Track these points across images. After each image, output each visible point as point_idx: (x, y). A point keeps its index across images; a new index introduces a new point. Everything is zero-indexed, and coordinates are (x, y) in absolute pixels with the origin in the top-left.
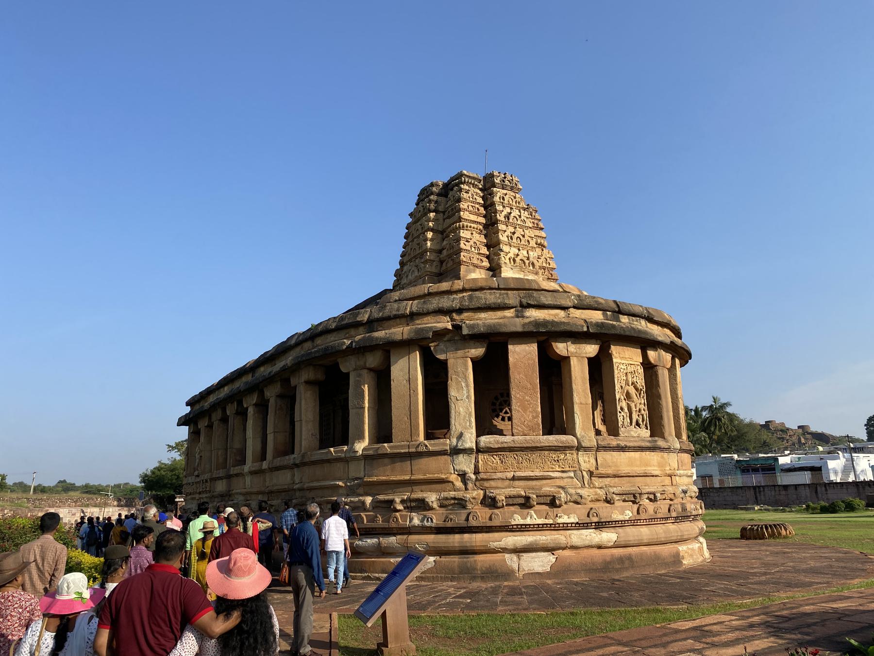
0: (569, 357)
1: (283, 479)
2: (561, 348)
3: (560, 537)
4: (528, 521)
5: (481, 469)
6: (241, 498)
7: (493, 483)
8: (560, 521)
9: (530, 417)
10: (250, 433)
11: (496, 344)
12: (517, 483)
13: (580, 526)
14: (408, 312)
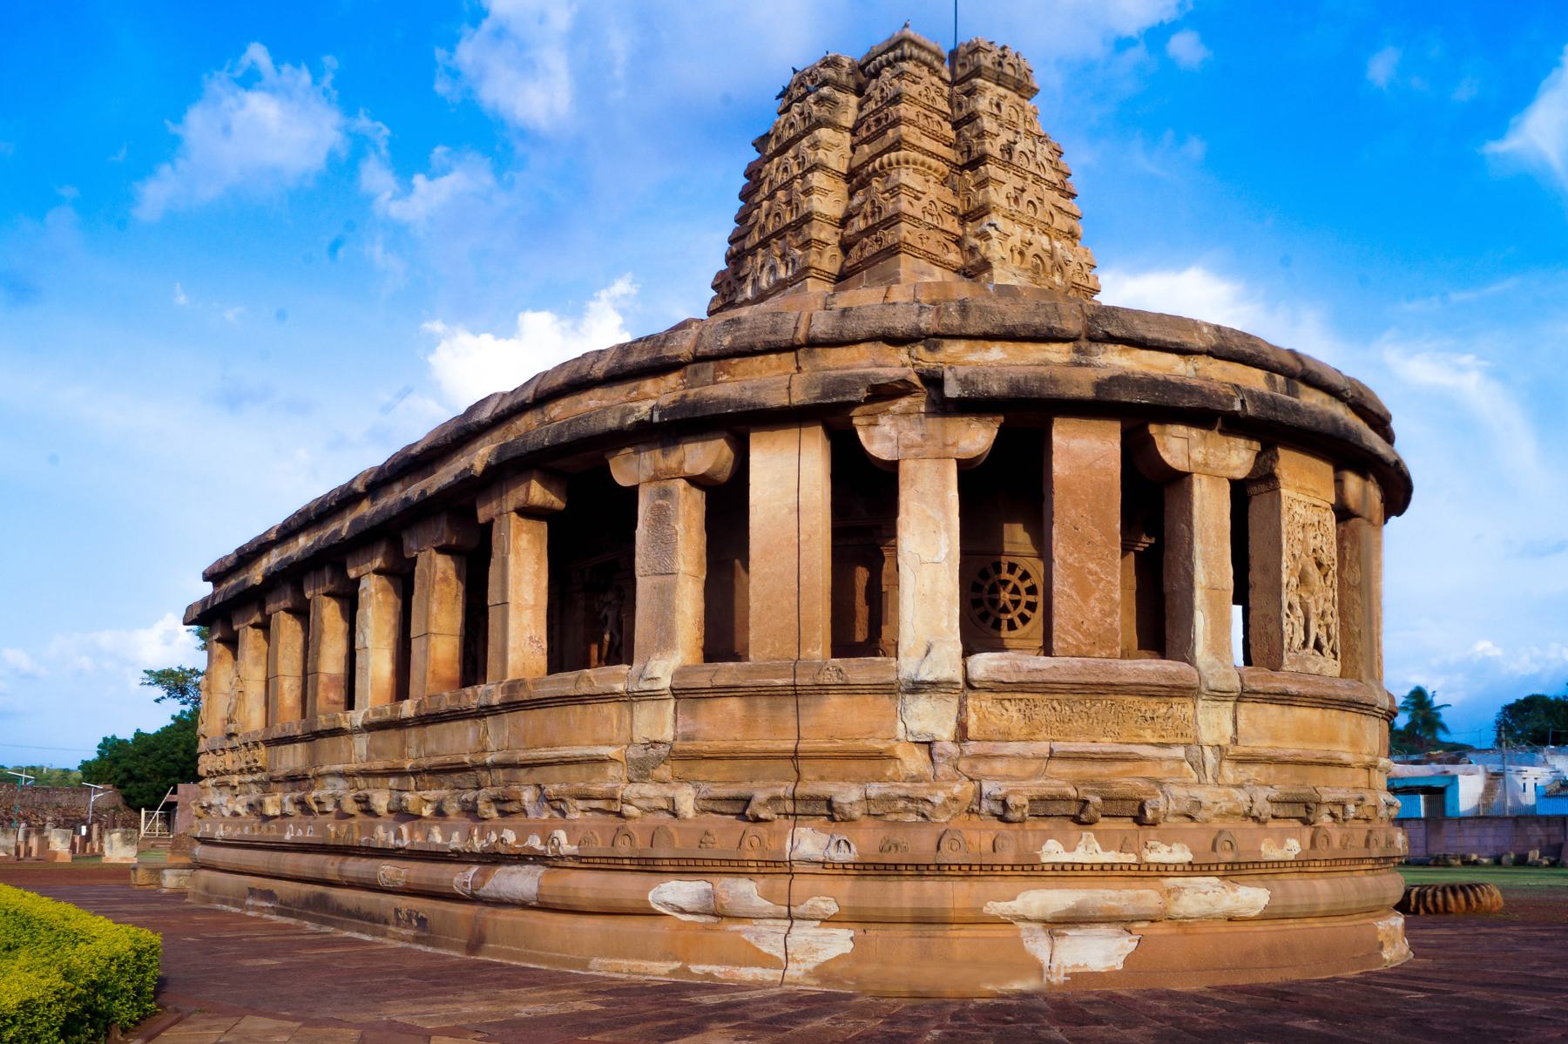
0: (1189, 475)
4: (1080, 856)
5: (972, 730)
7: (999, 767)
8: (1152, 857)
9: (1097, 614)
12: (1056, 767)
13: (1194, 869)
14: (801, 335)
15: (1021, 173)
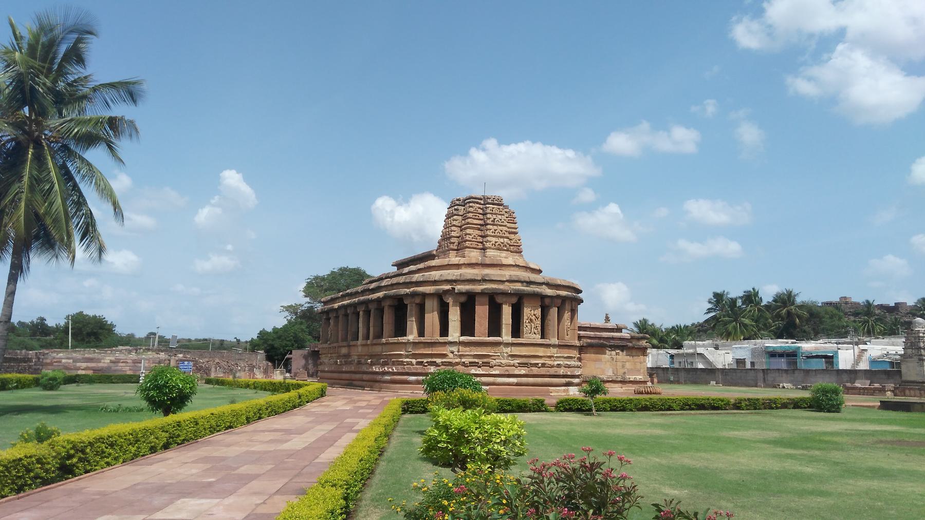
1: (378, 349)
2: (499, 300)
10: (361, 325)
15: (496, 225)
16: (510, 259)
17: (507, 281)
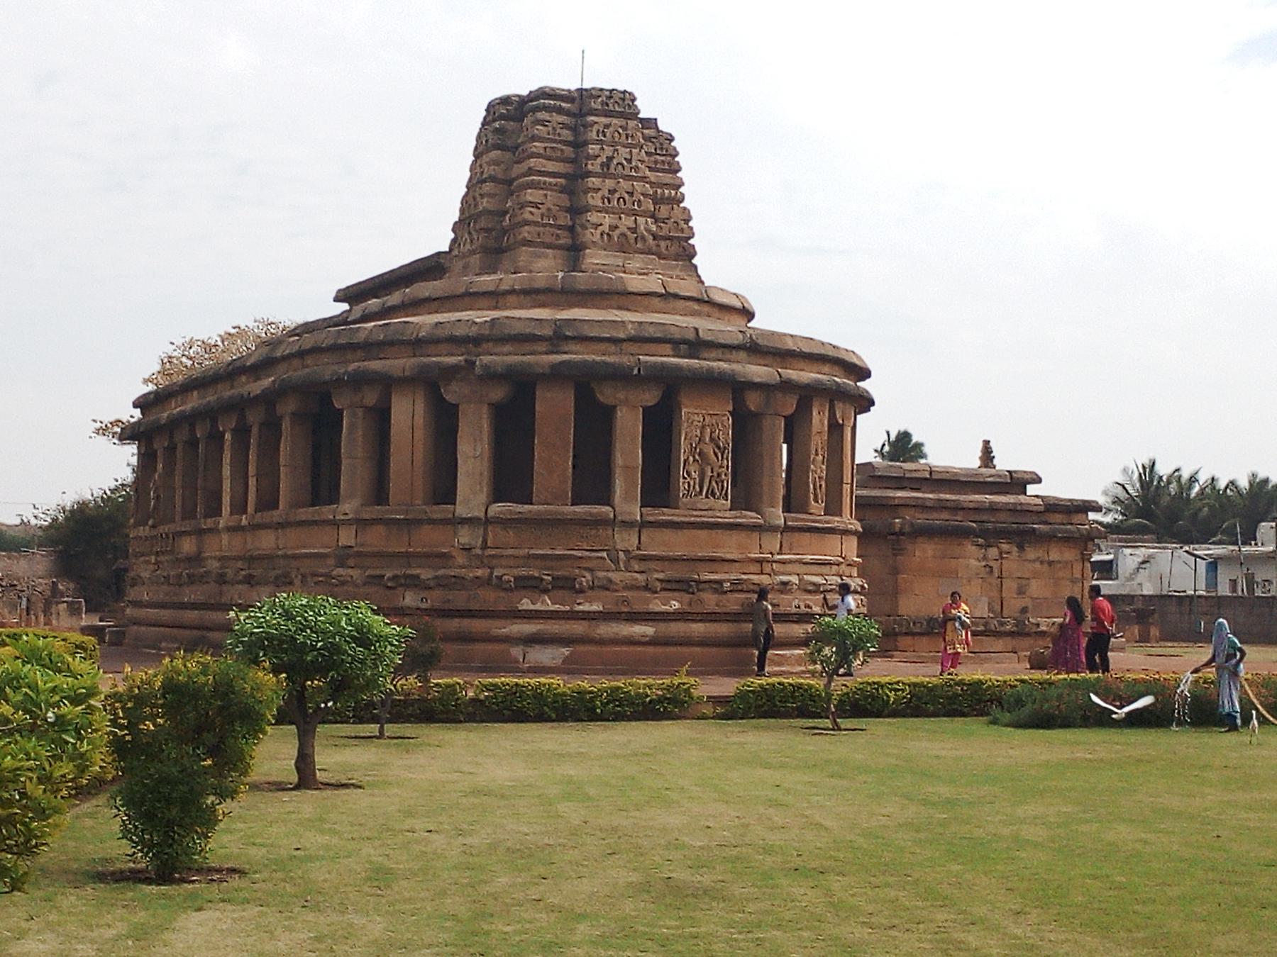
1: (266, 541)
2: (606, 394)
3: (578, 628)
4: (538, 607)
5: (489, 544)
6: (216, 564)
10: (226, 471)
11: (523, 387)
16: (643, 276)
17: (631, 339)
